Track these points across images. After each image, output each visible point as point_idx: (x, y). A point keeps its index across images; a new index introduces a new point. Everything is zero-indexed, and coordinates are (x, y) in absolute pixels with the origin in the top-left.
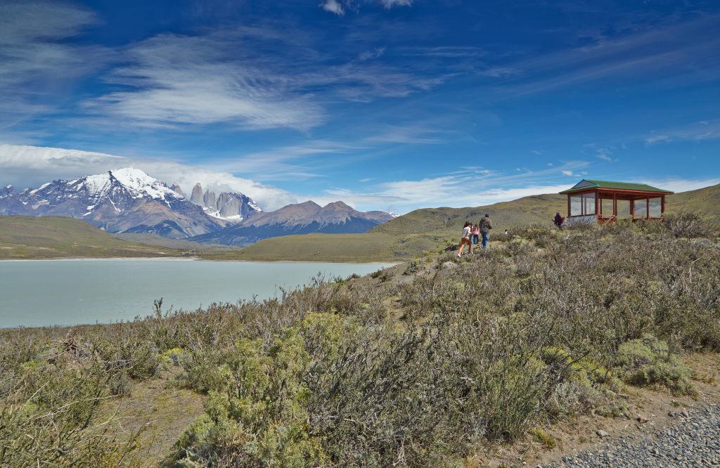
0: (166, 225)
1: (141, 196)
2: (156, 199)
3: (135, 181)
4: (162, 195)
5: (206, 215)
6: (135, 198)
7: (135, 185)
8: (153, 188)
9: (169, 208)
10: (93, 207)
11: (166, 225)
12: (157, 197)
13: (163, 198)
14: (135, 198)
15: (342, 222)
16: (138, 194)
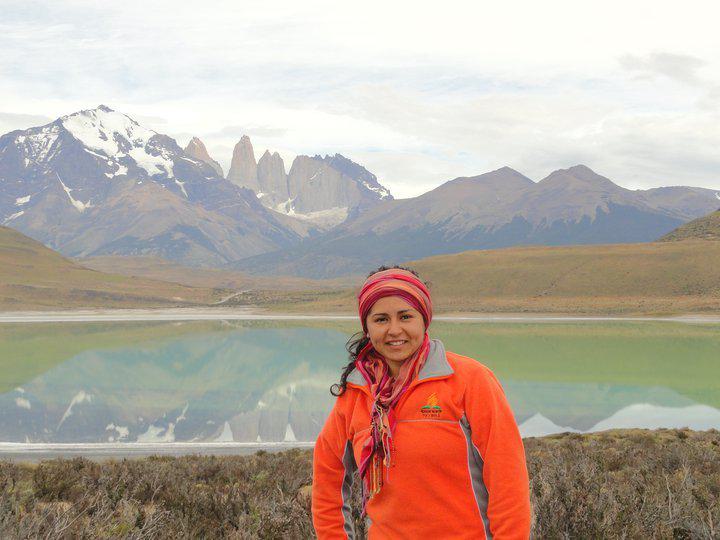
0: (178, 236)
1: (123, 171)
2: (156, 177)
3: (110, 137)
4: (169, 164)
5: (264, 210)
6: (110, 176)
7: (111, 147)
8: (148, 151)
9: (182, 195)
10: (27, 199)
11: (178, 236)
12: (159, 171)
13: (170, 176)
14: (110, 176)
15: (586, 218)
16: (117, 168)
